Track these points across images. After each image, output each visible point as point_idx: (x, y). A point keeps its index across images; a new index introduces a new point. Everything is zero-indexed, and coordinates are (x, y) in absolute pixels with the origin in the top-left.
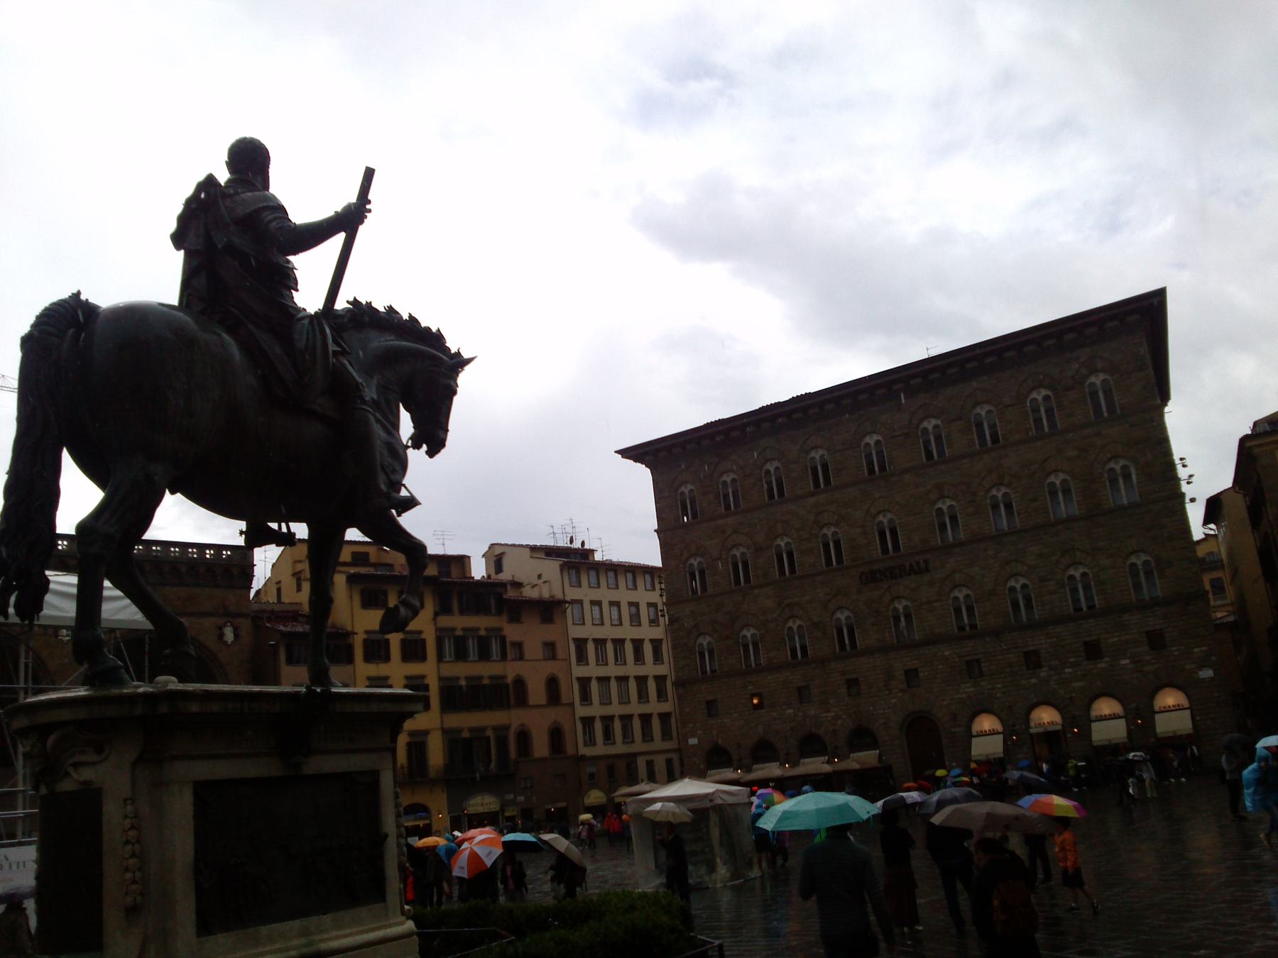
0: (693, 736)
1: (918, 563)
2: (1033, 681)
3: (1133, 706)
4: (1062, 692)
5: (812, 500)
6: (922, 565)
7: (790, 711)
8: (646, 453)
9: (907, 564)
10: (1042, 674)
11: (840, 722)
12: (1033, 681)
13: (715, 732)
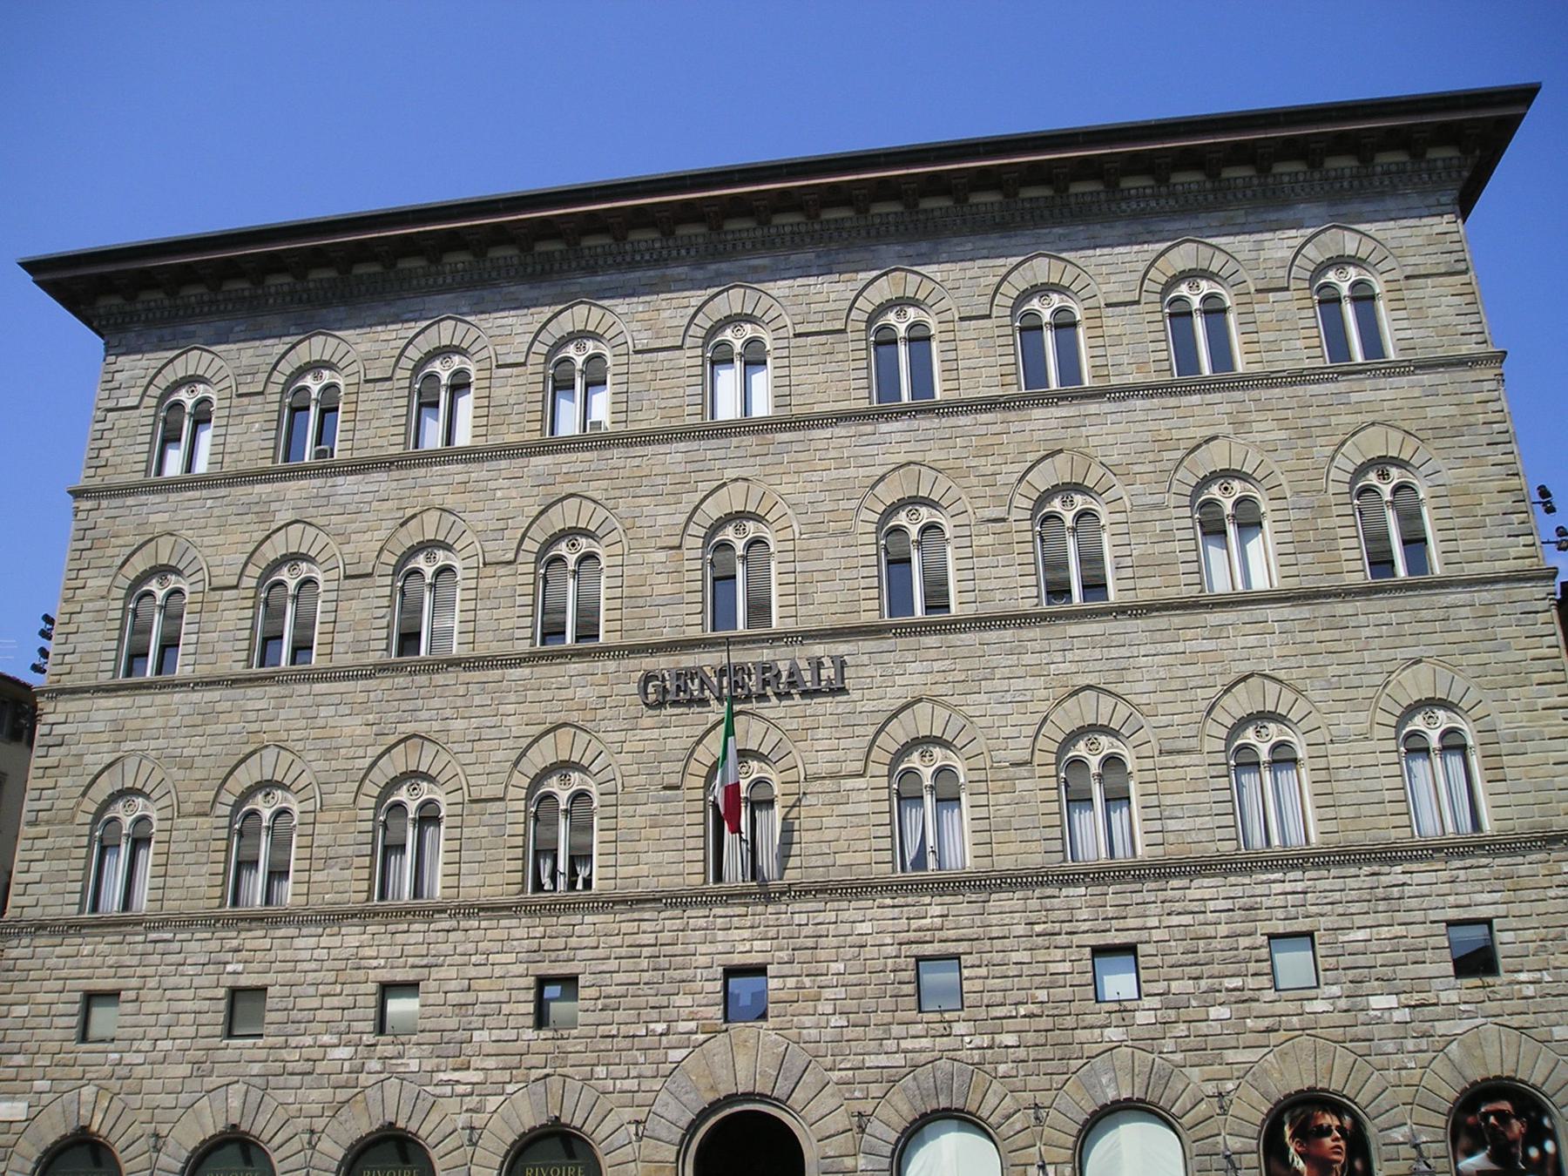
2: (1113, 1034)
6: (828, 673)
7: (345, 1052)
8: (105, 285)
9: (784, 667)
11: (492, 1103)
12: (1113, 1034)
13: (88, 1092)
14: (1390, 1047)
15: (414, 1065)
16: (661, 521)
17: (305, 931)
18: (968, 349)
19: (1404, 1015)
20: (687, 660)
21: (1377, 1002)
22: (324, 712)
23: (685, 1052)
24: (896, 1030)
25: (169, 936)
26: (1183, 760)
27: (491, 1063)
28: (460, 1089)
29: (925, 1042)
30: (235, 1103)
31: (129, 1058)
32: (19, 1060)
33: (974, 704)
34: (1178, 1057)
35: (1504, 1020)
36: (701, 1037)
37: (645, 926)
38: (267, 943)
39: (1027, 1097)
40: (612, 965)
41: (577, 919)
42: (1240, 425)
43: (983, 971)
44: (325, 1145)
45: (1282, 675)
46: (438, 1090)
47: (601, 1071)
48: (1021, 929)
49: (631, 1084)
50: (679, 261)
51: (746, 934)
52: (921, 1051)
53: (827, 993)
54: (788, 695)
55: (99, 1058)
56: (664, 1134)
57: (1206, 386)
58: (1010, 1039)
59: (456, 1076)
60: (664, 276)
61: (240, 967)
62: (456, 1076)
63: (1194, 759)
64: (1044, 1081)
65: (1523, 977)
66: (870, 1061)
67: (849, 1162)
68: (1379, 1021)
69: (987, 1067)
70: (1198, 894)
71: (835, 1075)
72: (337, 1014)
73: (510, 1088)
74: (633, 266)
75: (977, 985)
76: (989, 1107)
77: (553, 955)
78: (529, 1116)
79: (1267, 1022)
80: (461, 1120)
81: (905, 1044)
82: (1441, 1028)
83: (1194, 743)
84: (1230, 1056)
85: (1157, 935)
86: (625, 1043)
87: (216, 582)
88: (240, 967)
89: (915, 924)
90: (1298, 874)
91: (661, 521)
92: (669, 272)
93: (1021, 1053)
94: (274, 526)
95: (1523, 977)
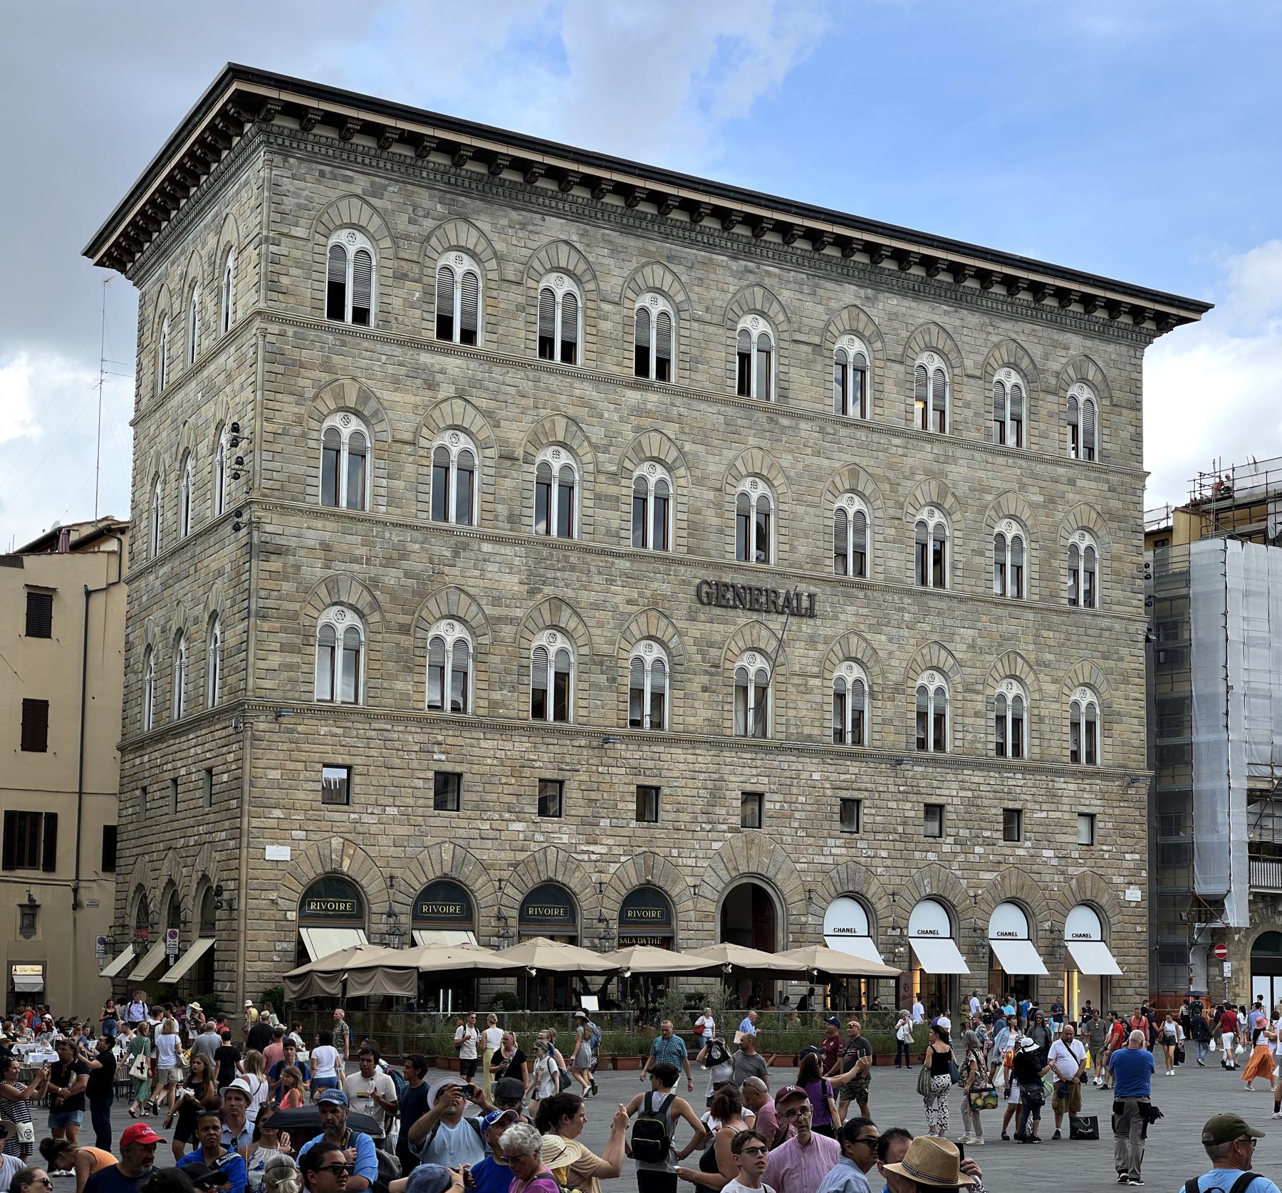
0: (276, 841)
1: (798, 596)
2: (931, 856)
3: (1047, 925)
4: (964, 882)
5: (633, 396)
6: (805, 603)
9: (782, 591)
10: (946, 848)
11: (613, 868)
12: (931, 856)
13: (336, 842)
14: (1047, 878)
15: (565, 839)
16: (711, 468)
17: (488, 736)
18: (889, 386)
19: (1055, 862)
20: (727, 579)
21: (1047, 853)
22: (491, 567)
23: (721, 844)
24: (831, 842)
25: (389, 727)
26: (974, 697)
27: (610, 841)
28: (593, 857)
29: (844, 851)
30: (447, 857)
31: (366, 818)
32: (277, 813)
33: (879, 640)
34: (959, 873)
35: (1095, 869)
36: (730, 835)
37: (700, 759)
38: (460, 741)
39: (890, 889)
40: (682, 782)
41: (661, 749)
42: (1023, 487)
43: (873, 811)
44: (509, 890)
45: (1023, 653)
46: (579, 857)
47: (675, 852)
48: (892, 788)
49: (691, 862)
50: (723, 250)
51: (754, 771)
52: (841, 855)
53: (797, 815)
54: (782, 613)
55: (344, 817)
56: (709, 895)
57: (1007, 454)
58: (884, 854)
59: (591, 848)
60: (711, 259)
61: (443, 757)
62: (591, 848)
63: (980, 698)
64: (898, 881)
65: (1105, 848)
66: (817, 859)
67: (803, 919)
68: (1045, 864)
69: (873, 869)
70: (976, 780)
71: (798, 866)
72: (513, 799)
73: (623, 859)
74: (693, 243)
75: (870, 819)
76: (872, 891)
77: (648, 772)
78: (634, 881)
79: (1000, 858)
80: (595, 877)
81: (834, 851)
82: (1071, 870)
83: (980, 687)
84: (983, 875)
85: (956, 801)
86: (690, 835)
87: (399, 436)
88: (443, 757)
89: (843, 777)
90: (1019, 776)
91: (711, 468)
92: (714, 256)
93: (889, 862)
94: (441, 396)
95: (1105, 848)
